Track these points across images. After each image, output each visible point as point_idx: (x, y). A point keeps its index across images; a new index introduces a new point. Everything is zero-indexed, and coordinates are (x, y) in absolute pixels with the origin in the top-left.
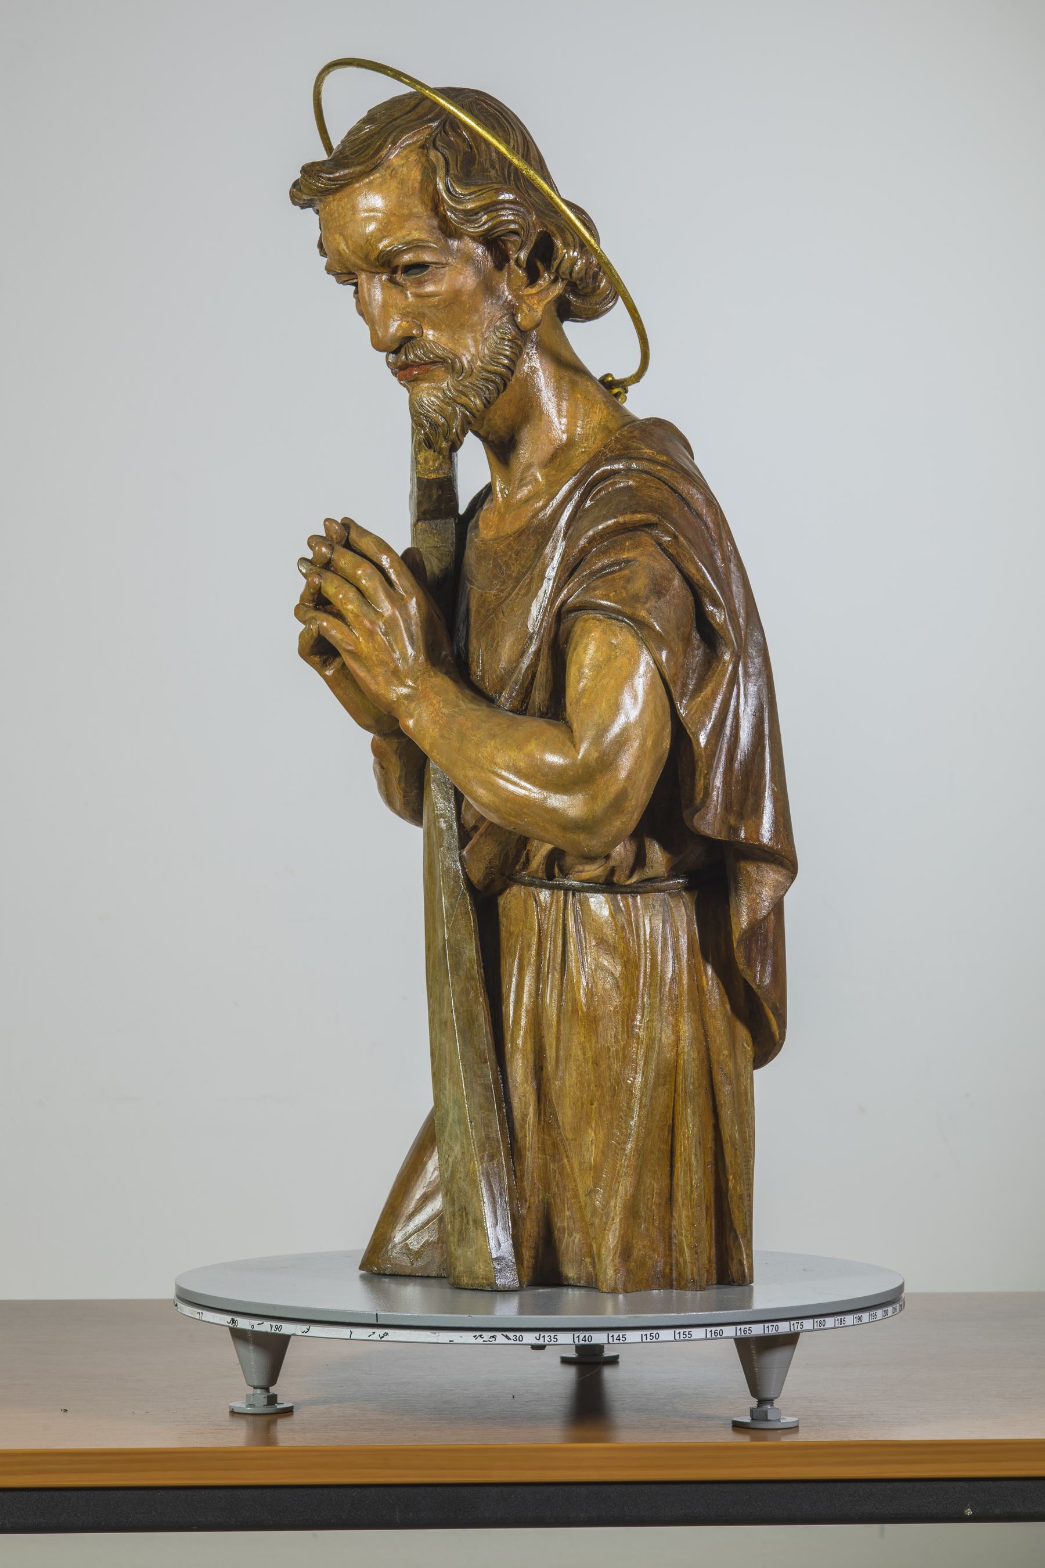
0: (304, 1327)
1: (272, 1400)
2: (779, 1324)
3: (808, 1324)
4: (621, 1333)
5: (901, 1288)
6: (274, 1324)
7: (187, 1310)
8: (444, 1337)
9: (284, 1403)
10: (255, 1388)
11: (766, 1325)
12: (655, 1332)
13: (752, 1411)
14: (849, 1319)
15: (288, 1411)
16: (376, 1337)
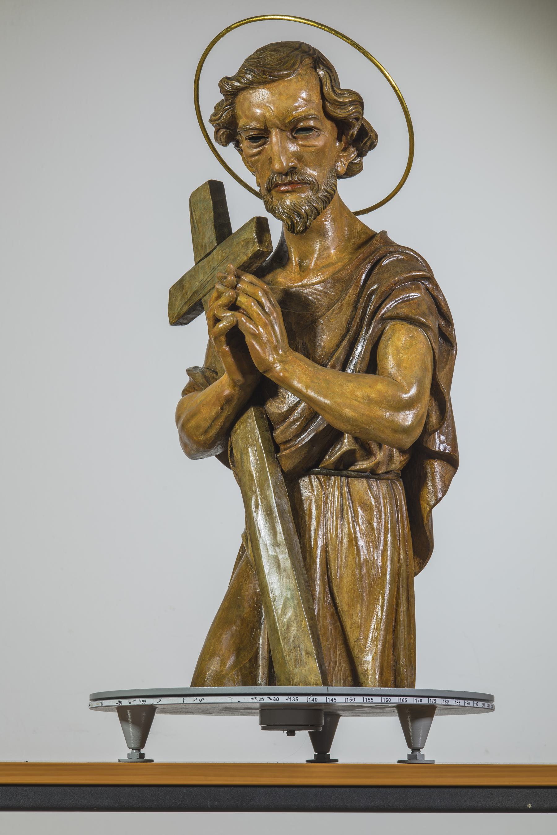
6: (141, 700)
8: (235, 699)
11: (415, 698)
16: (197, 701)
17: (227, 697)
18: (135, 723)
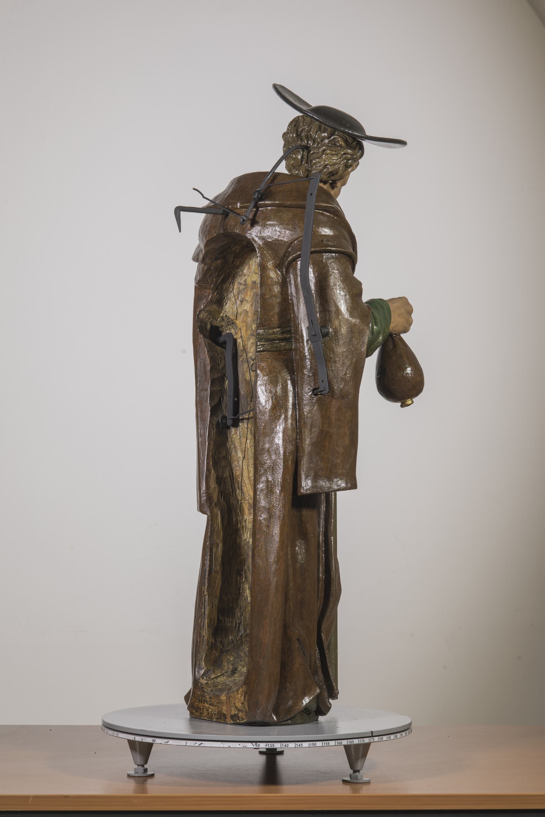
0: (166, 740)
1: (146, 770)
2: (365, 739)
3: (376, 739)
4: (301, 743)
5: (410, 724)
7: (110, 732)
8: (226, 745)
9: (149, 772)
10: (138, 765)
12: (314, 742)
13: (350, 776)
14: (392, 737)
15: (152, 776)
16: (197, 745)
17: (220, 743)
18: (141, 753)
